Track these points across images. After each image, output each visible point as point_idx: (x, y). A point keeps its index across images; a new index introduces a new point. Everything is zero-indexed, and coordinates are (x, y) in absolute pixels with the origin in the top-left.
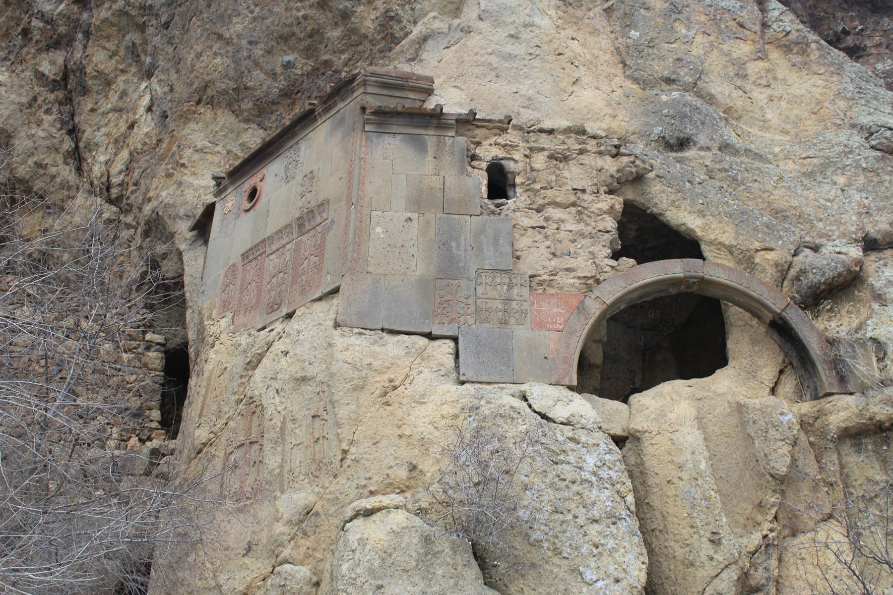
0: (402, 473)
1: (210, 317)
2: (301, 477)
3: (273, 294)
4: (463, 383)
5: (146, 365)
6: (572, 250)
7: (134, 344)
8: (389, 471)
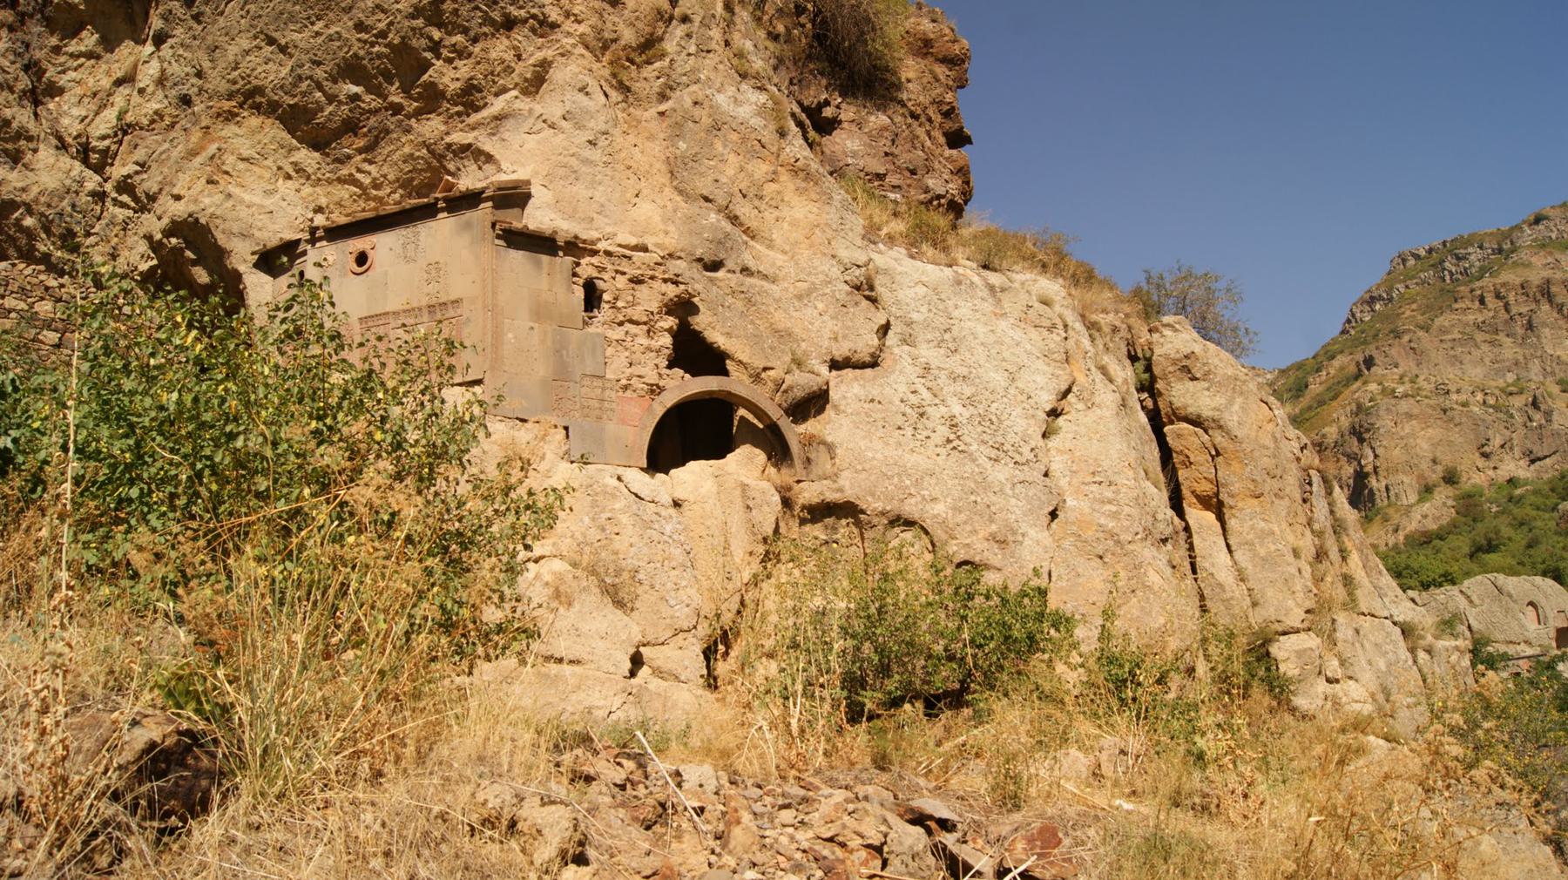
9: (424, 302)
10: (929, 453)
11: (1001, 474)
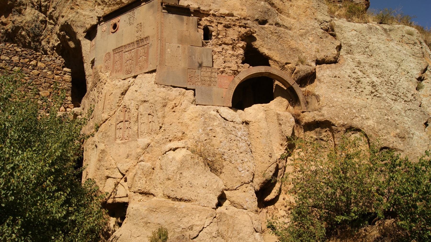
0: (180, 134)
1: (101, 71)
4: (197, 105)
7: (59, 72)
8: (175, 134)
9: (136, 39)
10: (363, 98)
11: (398, 106)
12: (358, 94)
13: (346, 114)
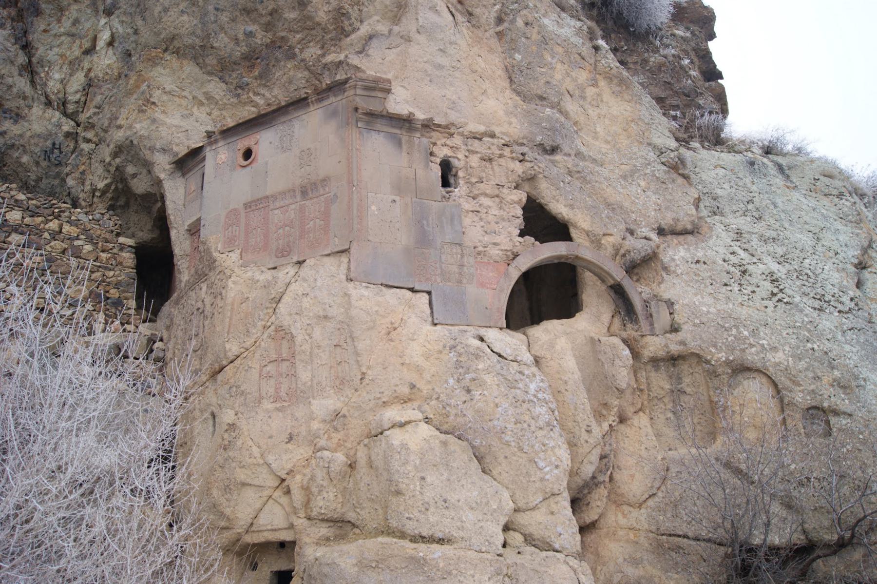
0: (405, 390)
2: (328, 389)
3: (281, 242)
4: (436, 325)
5: (121, 263)
6: (497, 229)
7: (111, 245)
11: (828, 322)
12: (746, 297)
13: (730, 339)
